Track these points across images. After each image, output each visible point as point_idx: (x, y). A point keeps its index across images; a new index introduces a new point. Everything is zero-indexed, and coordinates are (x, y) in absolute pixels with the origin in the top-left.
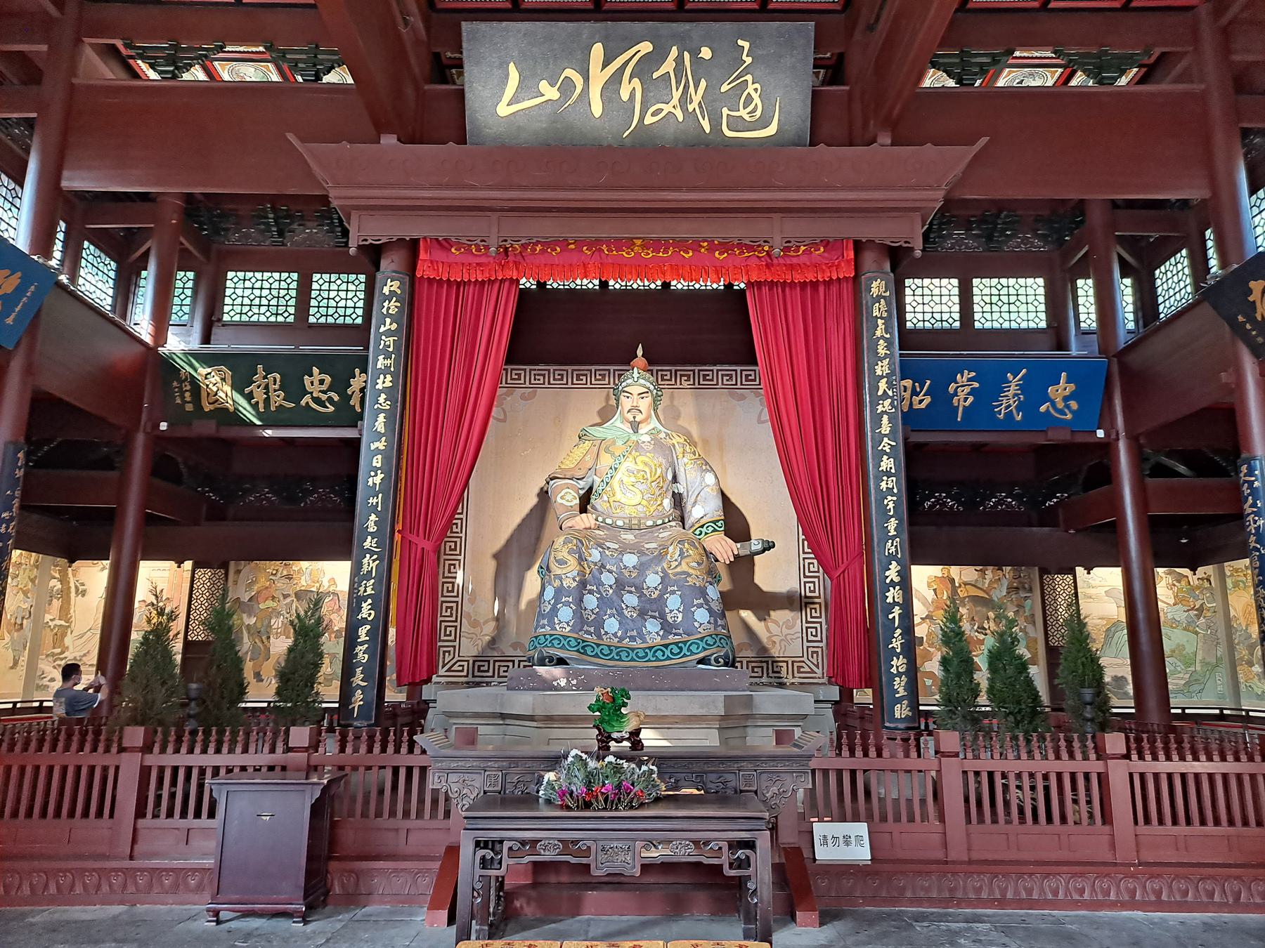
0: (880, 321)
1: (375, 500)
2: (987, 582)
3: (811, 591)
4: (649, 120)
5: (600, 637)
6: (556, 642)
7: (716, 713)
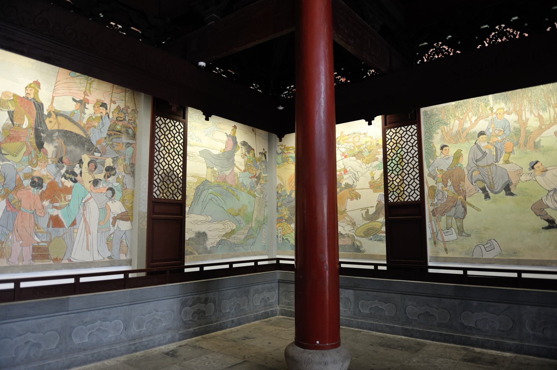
2: (86, 117)
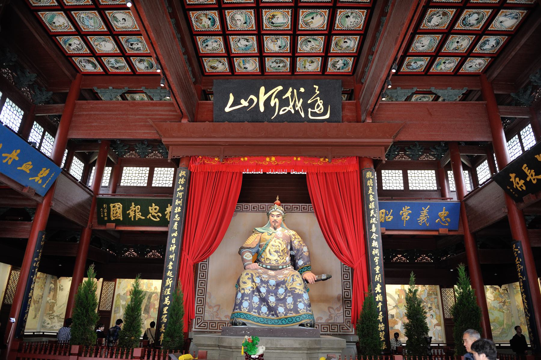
0: (370, 188)
1: (172, 256)
3: (347, 296)
4: (281, 113)
5: (259, 314)
6: (242, 316)
7: (305, 347)
